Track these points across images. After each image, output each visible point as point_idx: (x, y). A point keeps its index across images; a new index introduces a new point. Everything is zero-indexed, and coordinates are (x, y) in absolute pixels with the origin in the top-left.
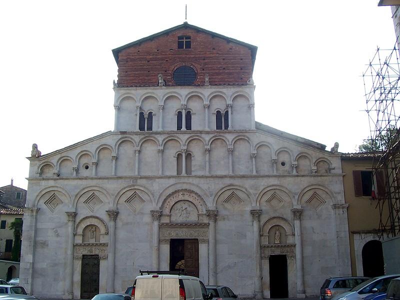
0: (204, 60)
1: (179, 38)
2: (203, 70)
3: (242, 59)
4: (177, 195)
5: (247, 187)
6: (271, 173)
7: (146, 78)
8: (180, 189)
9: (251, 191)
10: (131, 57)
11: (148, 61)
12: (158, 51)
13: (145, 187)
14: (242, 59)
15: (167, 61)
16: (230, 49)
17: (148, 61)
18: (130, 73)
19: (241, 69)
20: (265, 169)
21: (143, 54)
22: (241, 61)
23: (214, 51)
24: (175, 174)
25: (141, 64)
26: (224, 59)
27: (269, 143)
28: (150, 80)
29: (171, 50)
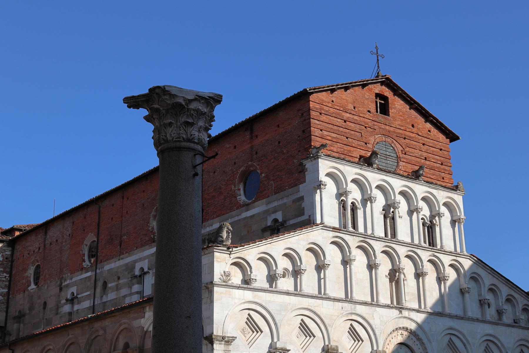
0: (405, 138)
1: (377, 95)
2: (405, 154)
3: (441, 150)
4: (395, 334)
5: (465, 333)
6: (479, 316)
7: (346, 148)
8: (401, 326)
9: (469, 339)
10: (326, 108)
11: (345, 121)
12: (354, 108)
13: (364, 318)
14: (441, 150)
15: (366, 127)
16: (429, 131)
17: (345, 121)
18: (325, 133)
19: (442, 164)
20: (473, 310)
21: (338, 108)
22: (441, 152)
23: (414, 130)
24: (389, 302)
25: (338, 124)
26: (424, 144)
27: (479, 275)
28: (350, 151)
29: (369, 111)
